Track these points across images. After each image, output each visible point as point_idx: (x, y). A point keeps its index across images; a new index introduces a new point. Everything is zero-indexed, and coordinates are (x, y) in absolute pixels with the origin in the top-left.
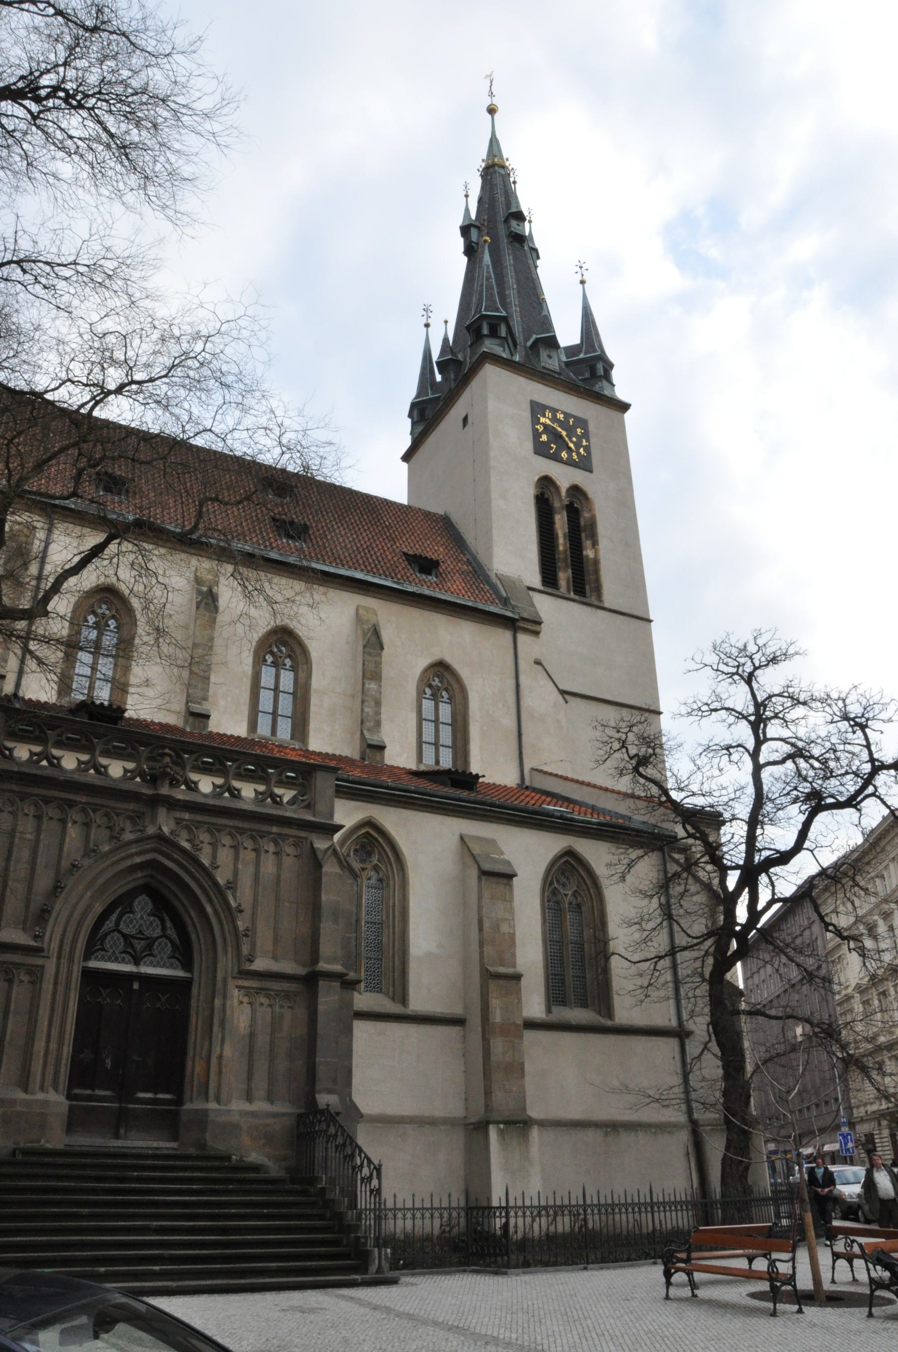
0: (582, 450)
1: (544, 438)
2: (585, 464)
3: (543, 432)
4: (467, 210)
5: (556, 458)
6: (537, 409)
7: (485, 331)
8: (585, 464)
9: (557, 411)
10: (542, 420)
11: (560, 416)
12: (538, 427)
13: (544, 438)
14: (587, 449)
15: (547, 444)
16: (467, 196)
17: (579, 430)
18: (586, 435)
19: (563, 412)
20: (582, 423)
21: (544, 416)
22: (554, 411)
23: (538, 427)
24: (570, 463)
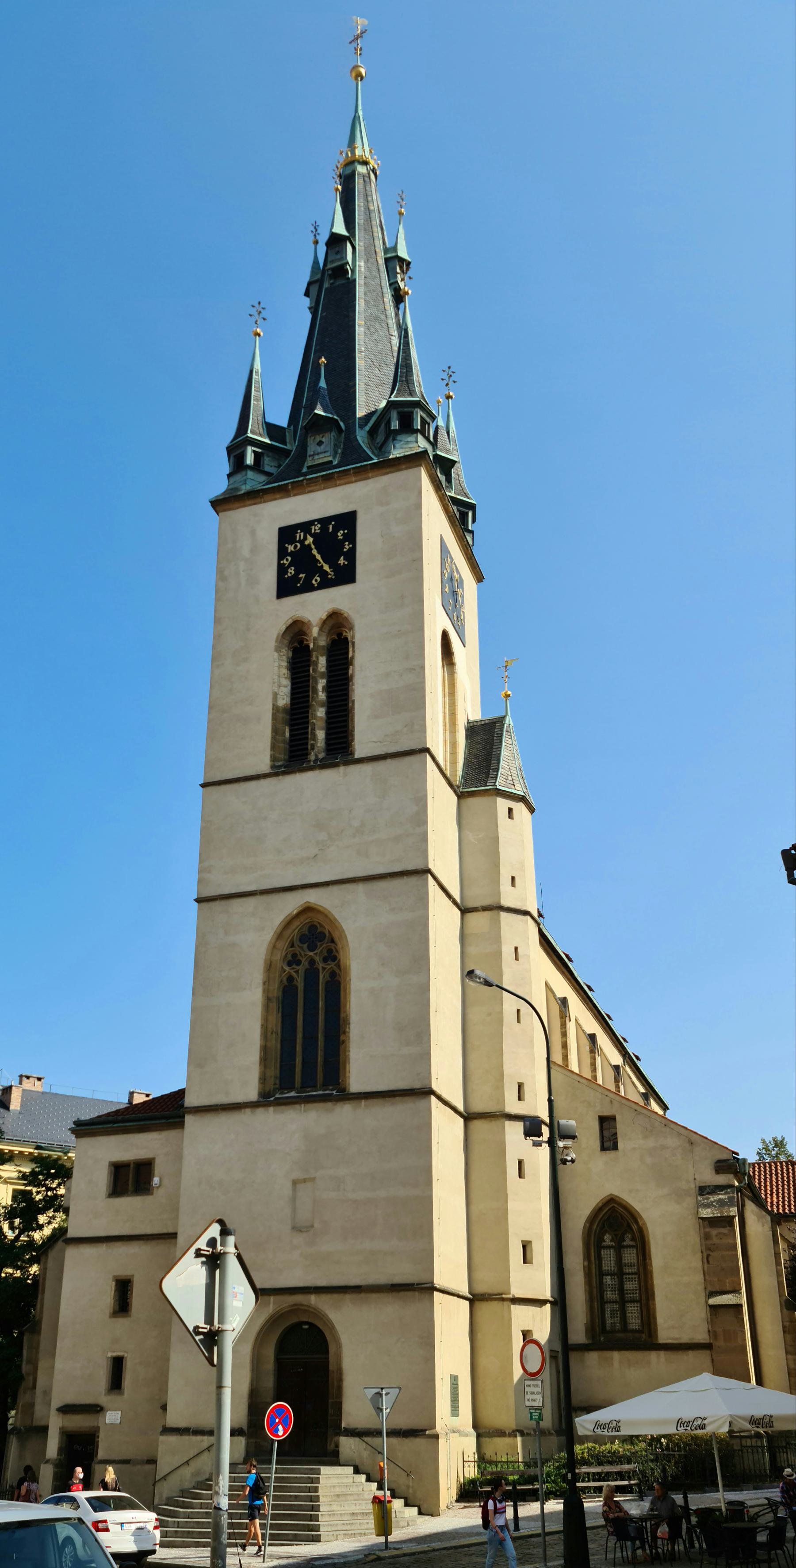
0: (342, 561)
1: (292, 571)
2: (346, 576)
3: (290, 565)
4: (316, 262)
5: (308, 588)
6: (286, 534)
7: (250, 459)
8: (346, 576)
9: (311, 523)
10: (291, 548)
11: (316, 529)
12: (285, 561)
13: (292, 571)
14: (351, 556)
15: (295, 578)
16: (316, 242)
17: (340, 534)
18: (351, 537)
19: (320, 521)
20: (348, 520)
21: (292, 541)
22: (305, 527)
23: (285, 561)
24: (326, 584)
